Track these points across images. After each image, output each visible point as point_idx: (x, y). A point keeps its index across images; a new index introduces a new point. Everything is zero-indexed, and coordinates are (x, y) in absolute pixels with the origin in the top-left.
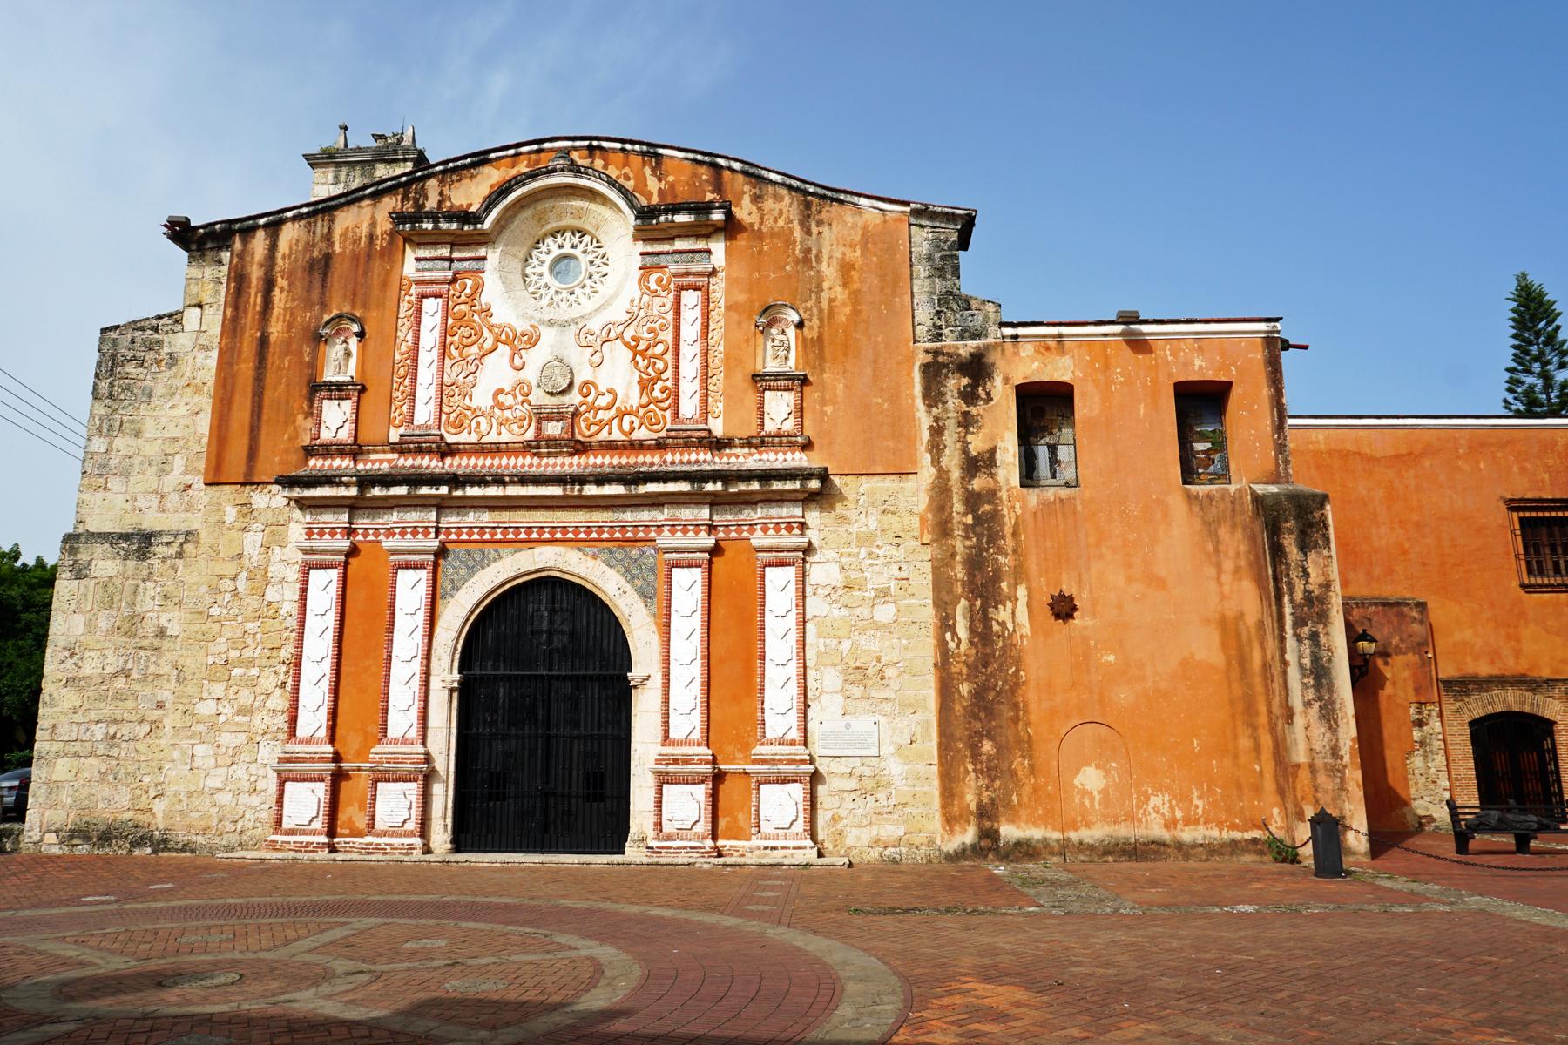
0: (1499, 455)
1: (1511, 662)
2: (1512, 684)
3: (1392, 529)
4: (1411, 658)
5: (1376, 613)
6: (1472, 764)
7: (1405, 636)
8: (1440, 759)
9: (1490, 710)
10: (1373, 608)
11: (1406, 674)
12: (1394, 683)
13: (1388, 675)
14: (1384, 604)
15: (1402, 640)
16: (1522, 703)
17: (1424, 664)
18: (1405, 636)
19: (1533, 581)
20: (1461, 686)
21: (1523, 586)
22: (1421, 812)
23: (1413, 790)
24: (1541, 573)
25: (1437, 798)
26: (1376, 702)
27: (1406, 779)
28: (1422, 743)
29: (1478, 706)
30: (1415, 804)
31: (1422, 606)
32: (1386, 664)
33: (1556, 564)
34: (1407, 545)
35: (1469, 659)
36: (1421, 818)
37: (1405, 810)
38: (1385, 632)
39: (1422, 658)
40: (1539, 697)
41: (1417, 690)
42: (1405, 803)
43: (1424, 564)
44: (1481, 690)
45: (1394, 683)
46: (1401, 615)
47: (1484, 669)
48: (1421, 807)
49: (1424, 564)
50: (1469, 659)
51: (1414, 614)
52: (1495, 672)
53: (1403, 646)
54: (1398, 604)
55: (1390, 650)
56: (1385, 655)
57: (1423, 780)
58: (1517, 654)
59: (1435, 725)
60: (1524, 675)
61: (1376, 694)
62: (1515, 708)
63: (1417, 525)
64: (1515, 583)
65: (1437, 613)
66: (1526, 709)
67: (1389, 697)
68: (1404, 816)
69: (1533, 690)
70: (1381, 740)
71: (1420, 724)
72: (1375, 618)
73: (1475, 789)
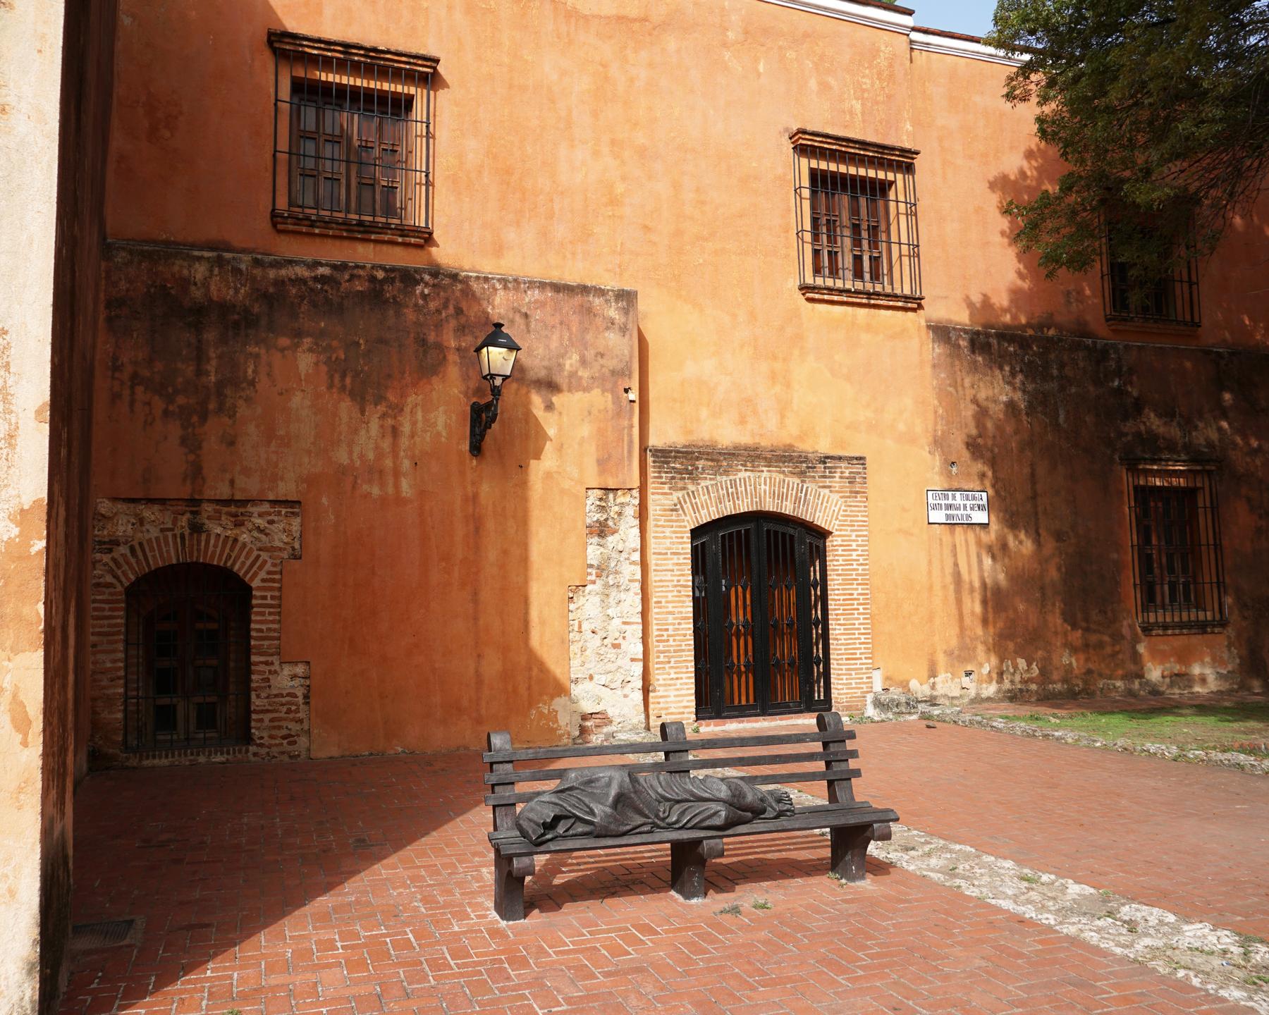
0: (791, 54)
1: (772, 423)
2: (769, 462)
3: (596, 153)
4: (599, 399)
5: (541, 305)
6: (688, 609)
7: (590, 354)
8: (632, 601)
9: (729, 509)
10: (535, 294)
11: (586, 430)
12: (560, 448)
13: (551, 432)
14: (557, 288)
15: (583, 362)
16: (782, 497)
17: (618, 414)
18: (590, 354)
19: (819, 281)
20: (684, 462)
21: (805, 288)
22: (588, 707)
23: (575, 663)
24: (834, 272)
25: (619, 677)
26: (524, 484)
27: (565, 643)
28: (601, 570)
29: (714, 500)
30: (576, 690)
31: (626, 298)
32: (549, 407)
33: (858, 260)
34: (620, 188)
35: (704, 413)
36: (585, 717)
37: (558, 703)
38: (554, 344)
39: (617, 400)
40: (810, 486)
41: (603, 464)
42: (560, 690)
43: (646, 228)
44: (717, 470)
45: (560, 448)
46: (588, 311)
47: (727, 434)
48: (586, 696)
49: (646, 228)
50: (704, 413)
51: (613, 312)
52: (745, 439)
53: (584, 374)
54: (584, 289)
55: (561, 380)
56: (550, 386)
57: (597, 640)
58: (783, 409)
59: (628, 532)
60: (790, 447)
61: (522, 467)
62: (770, 506)
63: (642, 152)
64: (794, 283)
65: (657, 316)
66: (788, 508)
67: (548, 475)
68: (553, 716)
69: (802, 474)
70: (525, 560)
71: (602, 530)
72: (538, 315)
73: (690, 656)
